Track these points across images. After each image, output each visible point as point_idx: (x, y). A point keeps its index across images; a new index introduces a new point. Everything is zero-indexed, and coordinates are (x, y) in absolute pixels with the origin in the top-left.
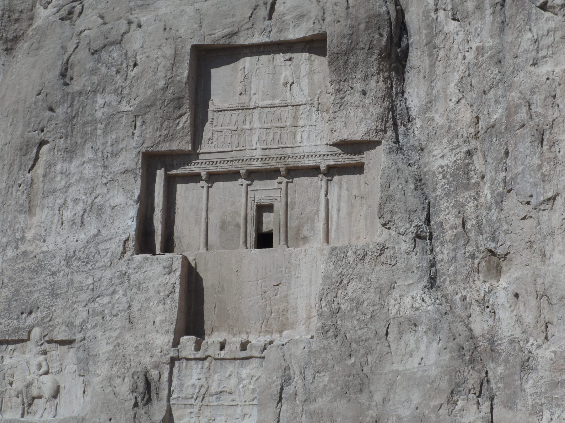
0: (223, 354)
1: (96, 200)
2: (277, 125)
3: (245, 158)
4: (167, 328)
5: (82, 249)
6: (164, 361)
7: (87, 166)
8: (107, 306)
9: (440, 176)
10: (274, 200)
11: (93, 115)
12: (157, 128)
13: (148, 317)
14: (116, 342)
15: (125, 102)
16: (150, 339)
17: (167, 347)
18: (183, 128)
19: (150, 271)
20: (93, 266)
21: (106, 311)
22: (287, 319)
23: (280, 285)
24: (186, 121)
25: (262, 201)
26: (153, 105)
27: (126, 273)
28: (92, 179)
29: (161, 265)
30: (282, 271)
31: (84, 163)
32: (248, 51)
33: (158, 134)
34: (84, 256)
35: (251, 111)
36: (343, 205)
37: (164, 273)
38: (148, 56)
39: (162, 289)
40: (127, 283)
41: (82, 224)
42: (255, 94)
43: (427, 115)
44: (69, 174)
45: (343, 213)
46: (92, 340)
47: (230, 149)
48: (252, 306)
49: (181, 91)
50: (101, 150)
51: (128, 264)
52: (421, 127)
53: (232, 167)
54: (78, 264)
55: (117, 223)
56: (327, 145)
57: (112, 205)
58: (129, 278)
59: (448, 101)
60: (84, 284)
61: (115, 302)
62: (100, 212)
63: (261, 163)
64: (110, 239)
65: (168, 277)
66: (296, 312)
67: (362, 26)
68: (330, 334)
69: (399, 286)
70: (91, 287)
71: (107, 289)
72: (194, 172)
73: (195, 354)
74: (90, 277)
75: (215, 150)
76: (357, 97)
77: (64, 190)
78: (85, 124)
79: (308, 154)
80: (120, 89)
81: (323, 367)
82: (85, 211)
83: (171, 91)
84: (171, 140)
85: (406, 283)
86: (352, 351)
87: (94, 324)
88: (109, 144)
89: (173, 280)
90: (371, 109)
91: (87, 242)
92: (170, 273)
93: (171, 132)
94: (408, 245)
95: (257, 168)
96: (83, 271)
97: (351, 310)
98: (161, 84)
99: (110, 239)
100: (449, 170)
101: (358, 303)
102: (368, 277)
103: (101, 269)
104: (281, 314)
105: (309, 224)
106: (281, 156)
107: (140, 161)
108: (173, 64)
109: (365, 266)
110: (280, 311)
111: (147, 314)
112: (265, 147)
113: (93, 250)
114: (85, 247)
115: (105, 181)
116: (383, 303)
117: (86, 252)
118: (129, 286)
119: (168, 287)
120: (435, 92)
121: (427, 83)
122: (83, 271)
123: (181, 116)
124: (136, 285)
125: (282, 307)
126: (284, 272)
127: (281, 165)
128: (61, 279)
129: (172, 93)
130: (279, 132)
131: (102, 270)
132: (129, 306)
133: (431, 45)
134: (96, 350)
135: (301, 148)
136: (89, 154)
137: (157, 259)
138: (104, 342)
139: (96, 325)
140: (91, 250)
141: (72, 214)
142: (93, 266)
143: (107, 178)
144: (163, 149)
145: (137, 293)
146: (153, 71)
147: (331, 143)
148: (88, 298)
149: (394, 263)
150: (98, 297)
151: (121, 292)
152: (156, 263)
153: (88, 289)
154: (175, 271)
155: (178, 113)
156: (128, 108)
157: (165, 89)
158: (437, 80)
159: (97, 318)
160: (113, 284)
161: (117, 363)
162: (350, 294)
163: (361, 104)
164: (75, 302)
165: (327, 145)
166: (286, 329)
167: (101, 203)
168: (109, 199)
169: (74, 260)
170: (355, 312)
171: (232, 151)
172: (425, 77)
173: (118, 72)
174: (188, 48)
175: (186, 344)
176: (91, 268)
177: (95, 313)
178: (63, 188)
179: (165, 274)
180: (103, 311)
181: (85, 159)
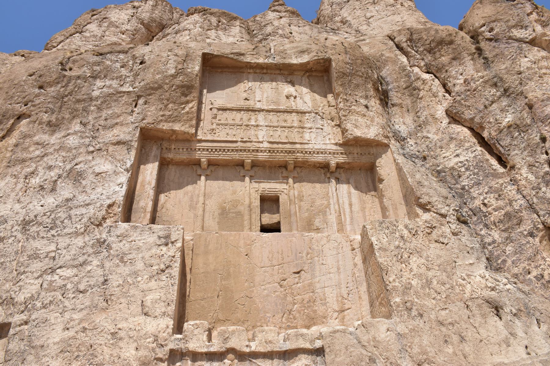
0: (254, 347)
1: (77, 167)
2: (285, 125)
4: (163, 310)
5: (48, 214)
6: (160, 356)
7: (71, 138)
8: (71, 279)
9: (463, 169)
11: (90, 94)
12: (161, 108)
13: (133, 296)
14: (81, 326)
15: (128, 85)
16: (136, 323)
18: (188, 113)
19: (139, 240)
20: (60, 232)
21: (69, 286)
23: (303, 272)
24: (192, 107)
25: (267, 192)
26: (160, 87)
27: (105, 241)
28: (75, 148)
30: (302, 257)
31: (68, 135)
32: (251, 71)
33: (161, 113)
34: (49, 221)
35: (257, 113)
37: (158, 243)
38: (158, 55)
39: (153, 261)
40: (105, 253)
41: (53, 190)
42: (259, 101)
43: (419, 135)
44: (48, 144)
46: (40, 324)
47: (235, 139)
48: (267, 295)
49: (192, 81)
50: (91, 123)
51: (109, 232)
53: (236, 156)
54: (38, 229)
55: (99, 190)
56: (336, 144)
57: (97, 172)
58: (109, 248)
59: (439, 123)
60: (42, 252)
61: (84, 274)
62: (79, 178)
64: (88, 205)
65: (164, 249)
66: (325, 304)
67: (359, 61)
68: (414, 313)
69: (460, 265)
70: (53, 254)
71: (75, 259)
73: (208, 347)
74: (53, 244)
75: (219, 139)
76: (362, 109)
77: (38, 159)
78: (78, 101)
80: (124, 77)
81: (425, 357)
82: (60, 177)
83: (181, 79)
84: (173, 121)
85: (467, 263)
86: (445, 336)
87: (47, 302)
88: (103, 118)
89: (171, 253)
90: (376, 119)
91: (56, 206)
93: (175, 114)
94: (455, 225)
96: (43, 238)
97: (423, 287)
98: (173, 71)
99: (88, 205)
100: (470, 164)
101: (427, 281)
103: (69, 236)
105: (321, 217)
107: (137, 135)
108: (184, 61)
111: (131, 291)
113: (63, 215)
114: (53, 211)
115: (91, 149)
116: (451, 282)
117: (53, 216)
118: (109, 256)
119: (165, 259)
120: (422, 118)
121: (412, 114)
122: (43, 238)
123: (187, 102)
124: (118, 255)
125: (307, 297)
126: (305, 258)
127: (289, 158)
128: (9, 245)
129: (181, 81)
130: (287, 131)
131: (70, 238)
132: (106, 280)
133: (411, 88)
134: (44, 339)
135: (310, 145)
136: (76, 127)
137: (150, 228)
138: (60, 327)
139: (51, 302)
140: (59, 215)
141: (42, 180)
142: (60, 232)
143: (94, 147)
144: (164, 128)
145: (118, 266)
146: (163, 63)
147: (341, 142)
148: (45, 268)
149: (446, 242)
150: (60, 267)
151: (96, 262)
153: (47, 257)
154: (172, 243)
155: (184, 99)
156: (131, 89)
157: (174, 76)
158: (421, 111)
159: (53, 293)
160: (84, 254)
161: (78, 356)
163: (367, 114)
164: (24, 272)
165: (336, 144)
166: (314, 324)
167: (82, 169)
168: (93, 166)
169: (33, 225)
172: (408, 110)
173: (122, 67)
174: (201, 53)
176: (56, 234)
177: (51, 288)
178: (36, 158)
179: (159, 245)
180: (65, 286)
181: (70, 131)
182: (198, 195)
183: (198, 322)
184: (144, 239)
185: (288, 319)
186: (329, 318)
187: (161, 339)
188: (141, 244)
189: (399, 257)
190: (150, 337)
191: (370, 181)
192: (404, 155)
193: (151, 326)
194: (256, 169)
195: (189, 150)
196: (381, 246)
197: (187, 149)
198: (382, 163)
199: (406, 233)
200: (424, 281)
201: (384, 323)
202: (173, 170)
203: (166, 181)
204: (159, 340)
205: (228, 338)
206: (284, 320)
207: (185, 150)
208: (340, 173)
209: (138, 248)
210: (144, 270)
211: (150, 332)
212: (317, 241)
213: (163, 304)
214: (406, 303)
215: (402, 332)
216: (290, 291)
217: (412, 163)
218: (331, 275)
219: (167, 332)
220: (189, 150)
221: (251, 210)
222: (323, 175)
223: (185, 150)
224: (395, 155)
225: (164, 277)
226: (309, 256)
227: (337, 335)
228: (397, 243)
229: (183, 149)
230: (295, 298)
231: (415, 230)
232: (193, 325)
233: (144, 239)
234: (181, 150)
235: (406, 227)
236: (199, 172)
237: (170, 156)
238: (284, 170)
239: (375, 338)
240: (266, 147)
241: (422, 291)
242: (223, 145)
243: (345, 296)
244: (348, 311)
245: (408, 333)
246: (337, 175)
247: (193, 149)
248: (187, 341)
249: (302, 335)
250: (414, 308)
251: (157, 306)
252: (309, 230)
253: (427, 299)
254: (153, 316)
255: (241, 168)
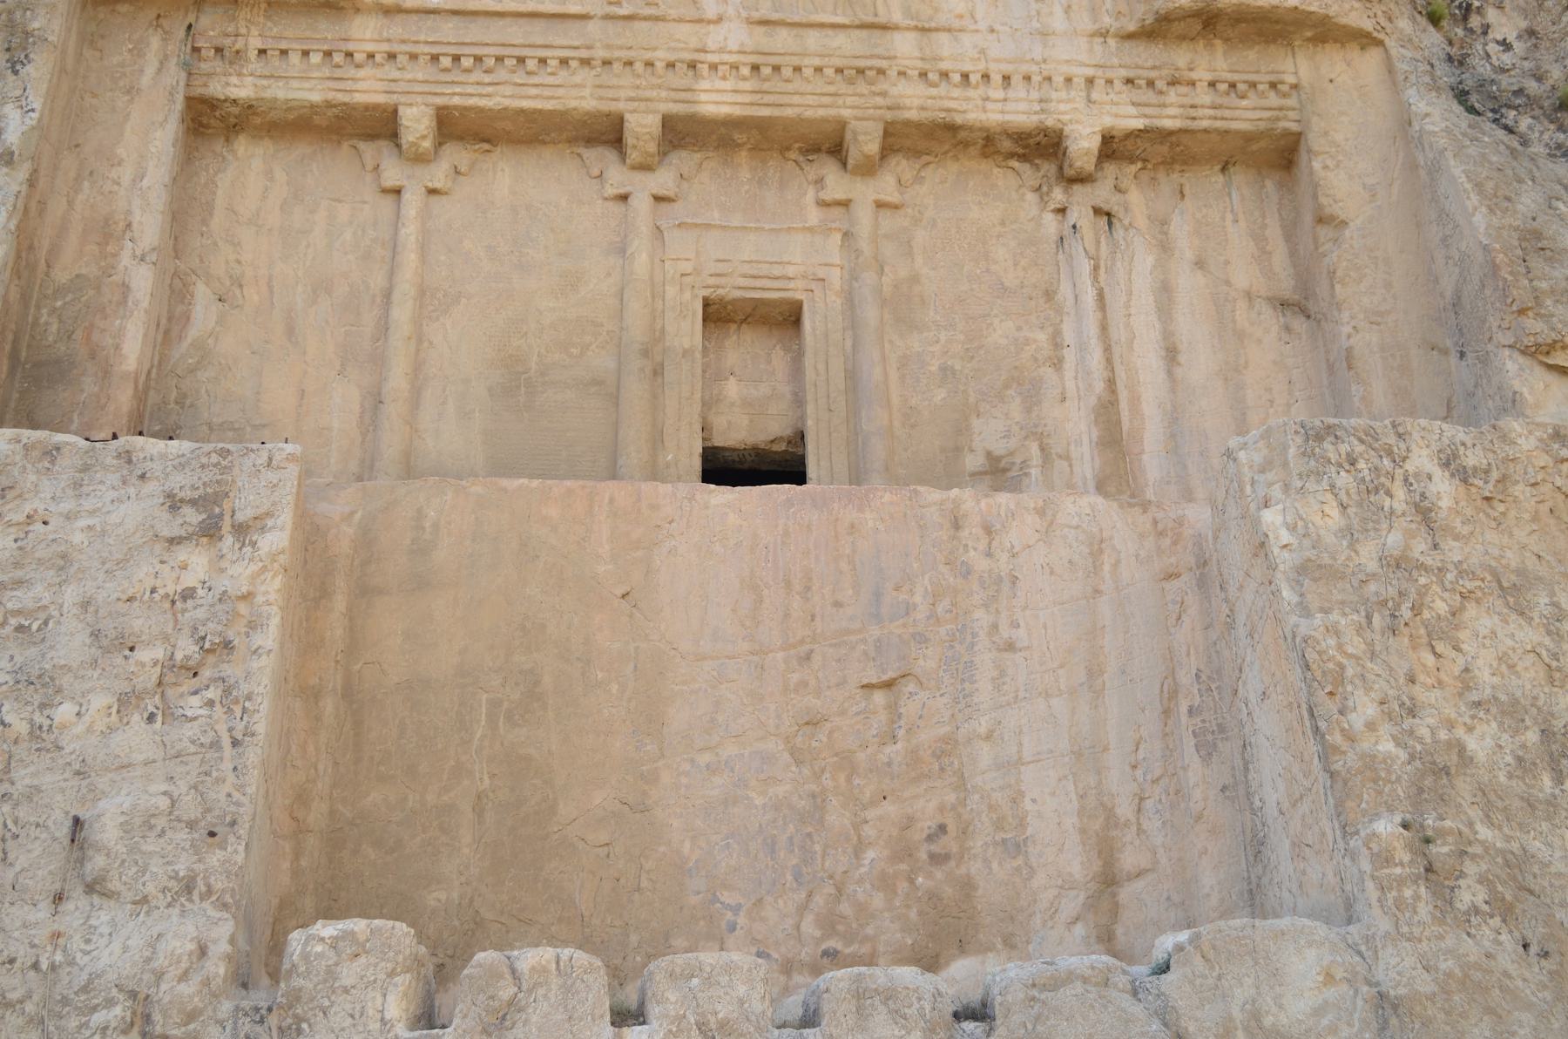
3: (660, 54)
10: (800, 284)
17: (186, 989)
19: (68, 517)
22: (967, 886)
29: (150, 487)
36: (1192, 328)
37: (166, 533)
39: (139, 622)
45: (1200, 363)
52: (1531, 33)
56: (1104, 34)
63: (747, 86)
68: (1470, 894)
72: (359, 98)
79: (1007, 68)
92: (210, 531)
95: (725, 110)
102: (1552, 594)
104: (924, 856)
105: (1015, 408)
106: (862, 63)
109: (1520, 535)
110: (918, 835)
112: (775, 16)
119: (200, 614)
126: (921, 614)
135: (966, 39)
137: (127, 457)
147: (1132, 27)
152: (113, 479)
154: (241, 530)
162: (1484, 675)
166: (962, 948)
170: (1547, 781)
171: (584, 17)
175: (331, 973)
179: (173, 541)
182: (388, 295)
183: (359, 925)
184: (92, 513)
185: (829, 924)
186: (1038, 920)
187: (165, 1015)
188: (78, 538)
189: (1406, 613)
190: (110, 1003)
191: (1274, 232)
192: (1461, 96)
193: (116, 946)
194: (683, 160)
195: (338, 58)
196: (1311, 554)
197: (328, 54)
198: (1339, 137)
199: (1443, 489)
200: (1532, 736)
201: (1310, 944)
202: (257, 164)
203: (217, 222)
204: (157, 1017)
205: (511, 1003)
206: (809, 927)
207: (316, 58)
208: (1118, 189)
209: (64, 556)
210: (94, 663)
211: (111, 976)
212: (988, 530)
213: (182, 835)
214: (1428, 841)
215: (1402, 991)
216: (842, 778)
217: (1501, 134)
218: (1054, 702)
219: (196, 979)
220: (338, 58)
221: (658, 372)
222: (1031, 197)
223: (316, 58)
224: (1411, 94)
225: (195, 701)
226: (944, 605)
227: (1067, 995)
228: (1394, 539)
229: (306, 53)
230: (871, 814)
231: (1495, 475)
232: (334, 943)
233: (92, 513)
234: (295, 58)
235: (1449, 460)
236: (393, 173)
237: (239, 87)
238: (829, 169)
239: (1256, 1016)
240: (735, 48)
241: (1518, 786)
242: (515, 33)
243: (1125, 810)
244: (1139, 885)
245: (1432, 998)
246: (1101, 193)
247: (359, 57)
248: (299, 1019)
249: (889, 995)
250: (1471, 868)
251: (150, 846)
252: (949, 477)
253: (1545, 826)
254: (129, 896)
255: (610, 155)
